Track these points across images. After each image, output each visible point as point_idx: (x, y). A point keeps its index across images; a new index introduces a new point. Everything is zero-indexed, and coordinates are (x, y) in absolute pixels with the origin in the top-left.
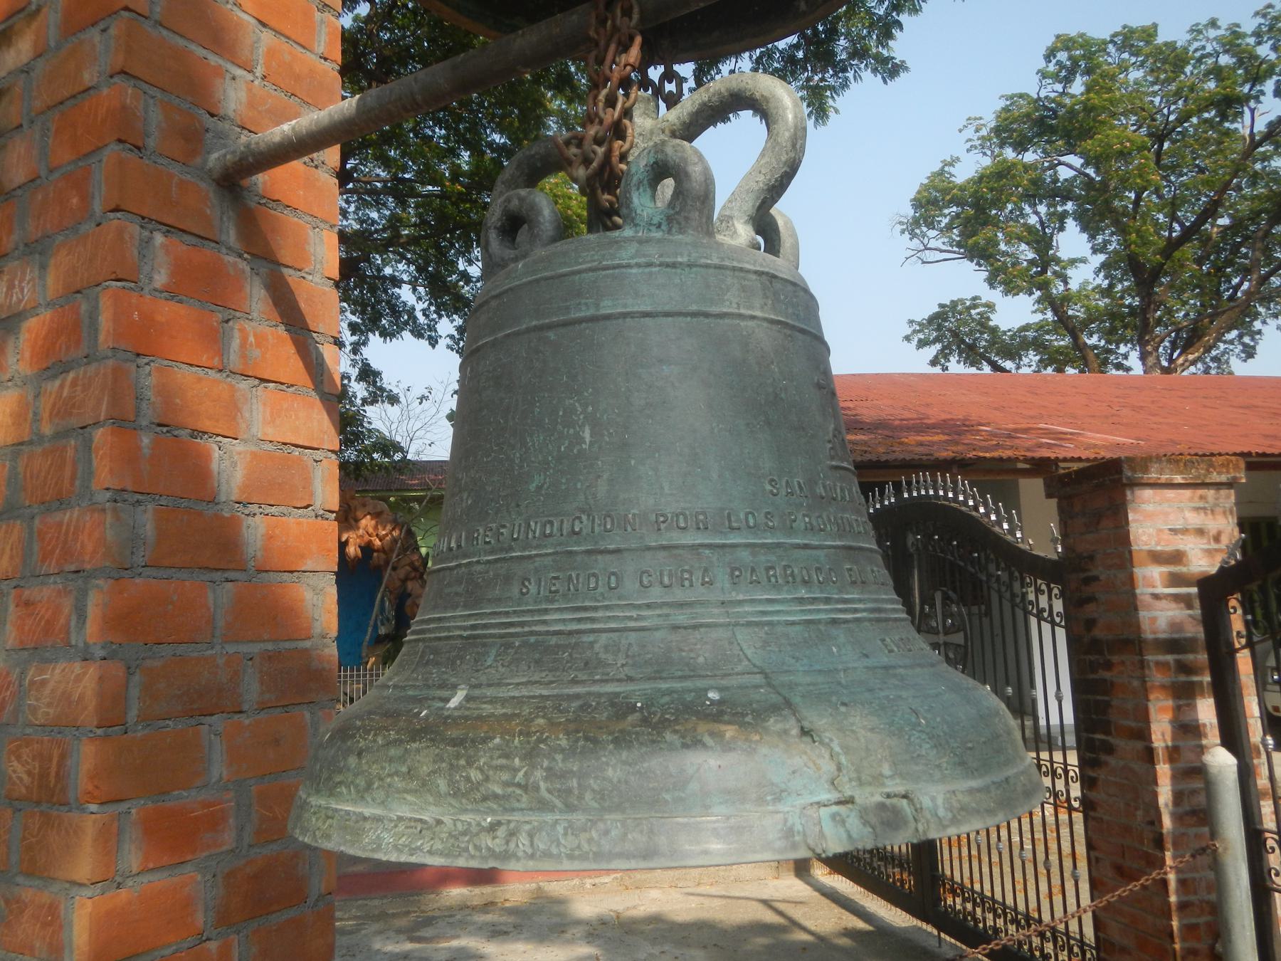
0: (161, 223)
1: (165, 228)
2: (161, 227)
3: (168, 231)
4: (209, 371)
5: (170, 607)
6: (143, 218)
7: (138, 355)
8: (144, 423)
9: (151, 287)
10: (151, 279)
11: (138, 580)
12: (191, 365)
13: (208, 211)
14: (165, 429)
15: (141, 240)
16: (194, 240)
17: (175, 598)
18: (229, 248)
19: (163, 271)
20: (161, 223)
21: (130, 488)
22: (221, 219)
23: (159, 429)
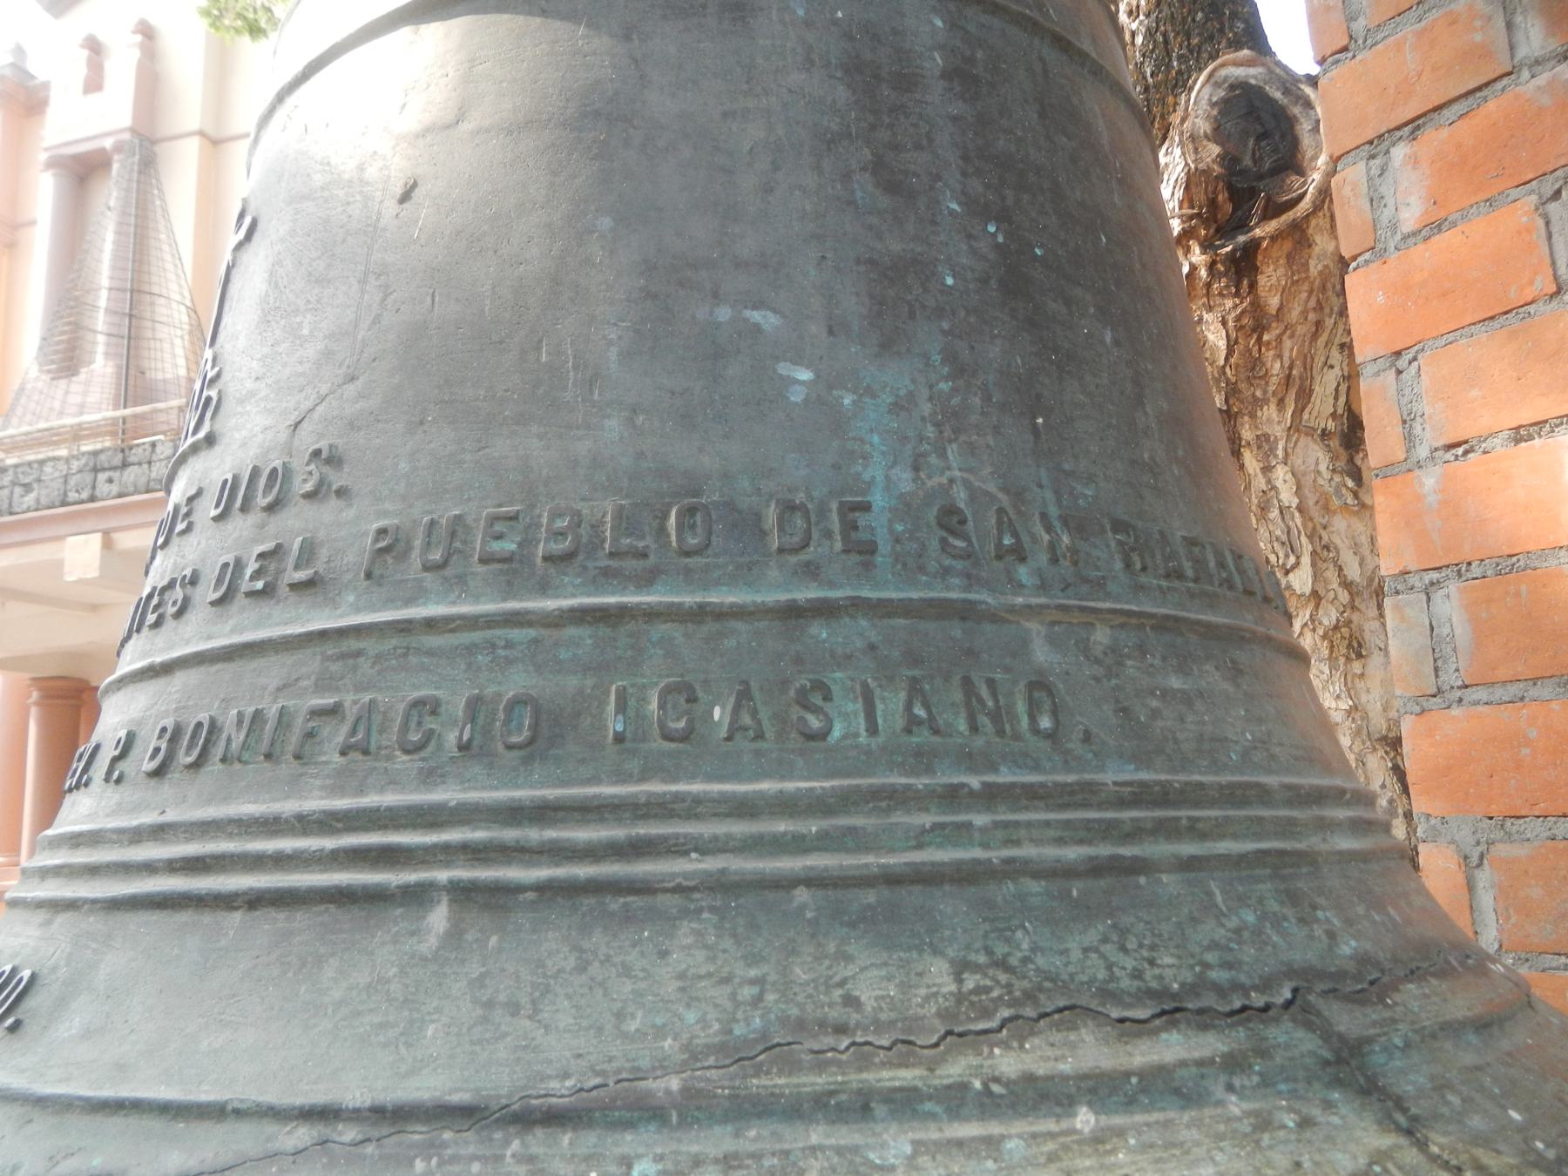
0: (1398, 128)
1: (1407, 130)
2: (1398, 134)
3: (1418, 128)
4: (1532, 308)
5: (1525, 751)
6: (1371, 142)
7: (1398, 354)
8: (1422, 452)
9: (1398, 237)
10: (1394, 227)
11: (1456, 711)
12: (1492, 318)
13: (1478, 37)
14: (1460, 451)
15: (1370, 179)
16: (1458, 108)
17: (1533, 733)
18: (1537, 62)
19: (1413, 200)
20: (1398, 128)
21: (1412, 568)
22: (1509, 26)
23: (1449, 456)
